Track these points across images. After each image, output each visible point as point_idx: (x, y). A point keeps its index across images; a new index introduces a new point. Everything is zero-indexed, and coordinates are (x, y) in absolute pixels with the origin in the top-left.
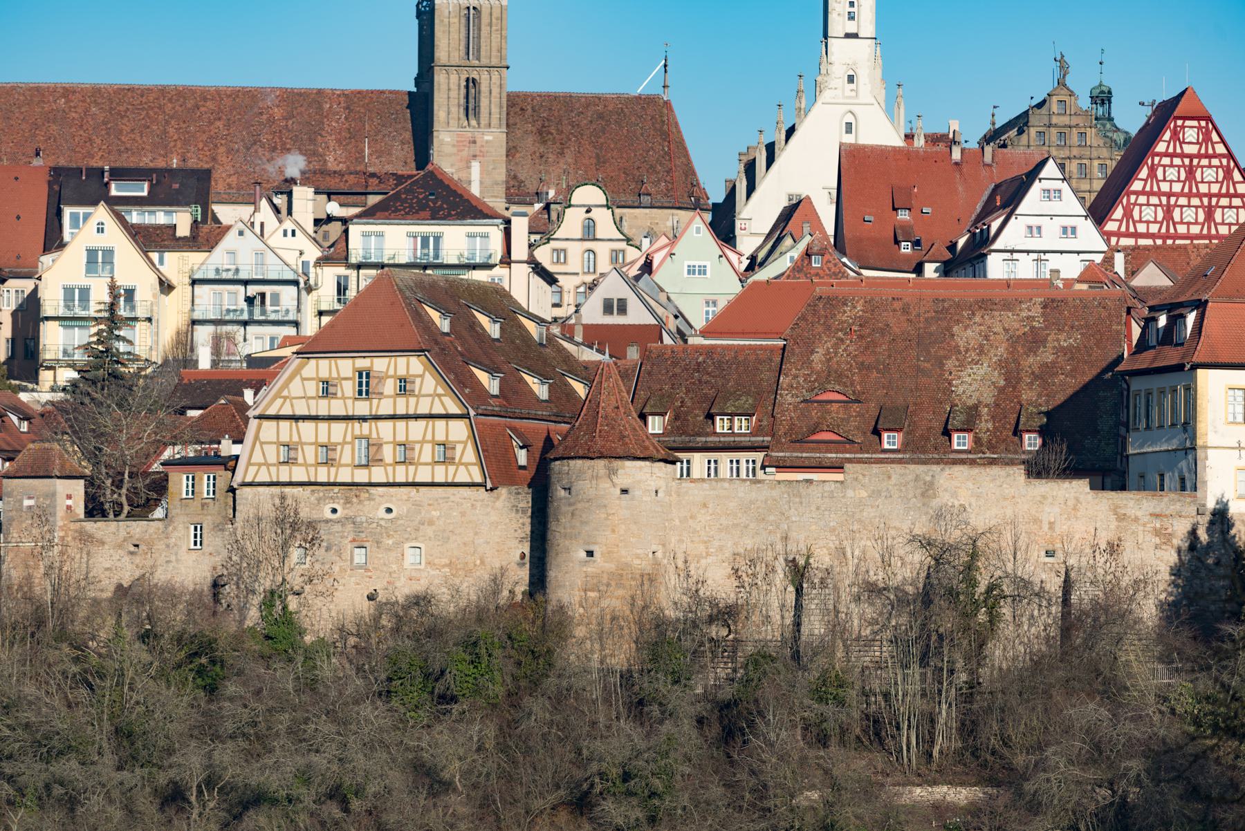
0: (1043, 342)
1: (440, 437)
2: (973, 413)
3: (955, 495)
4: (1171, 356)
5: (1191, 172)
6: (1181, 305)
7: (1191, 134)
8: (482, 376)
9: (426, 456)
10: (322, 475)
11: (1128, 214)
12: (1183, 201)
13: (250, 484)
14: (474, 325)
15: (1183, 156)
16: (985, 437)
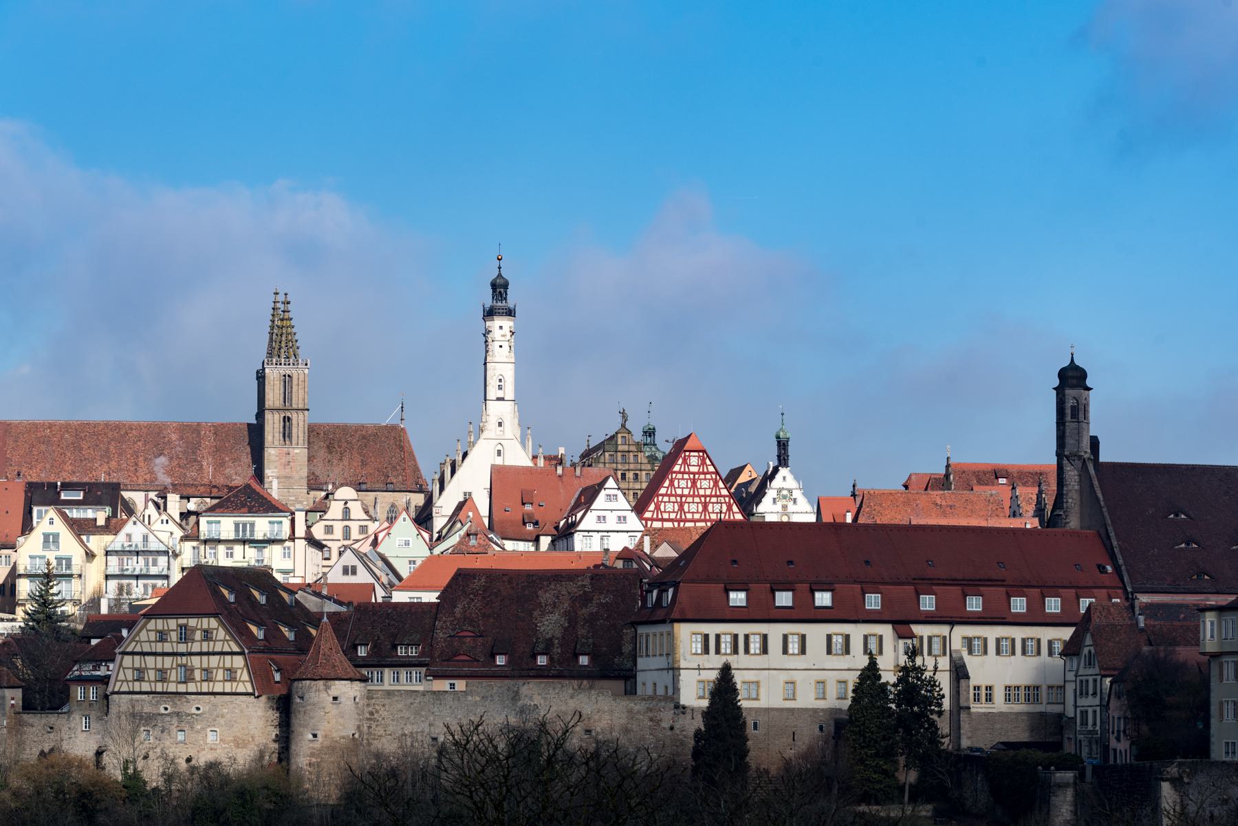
0: (592, 600)
1: (228, 665)
2: (549, 643)
3: (531, 698)
5: (694, 482)
6: (665, 583)
7: (694, 461)
8: (254, 629)
9: (220, 676)
10: (159, 687)
11: (657, 507)
12: (690, 500)
13: (118, 693)
15: (689, 473)
16: (556, 657)
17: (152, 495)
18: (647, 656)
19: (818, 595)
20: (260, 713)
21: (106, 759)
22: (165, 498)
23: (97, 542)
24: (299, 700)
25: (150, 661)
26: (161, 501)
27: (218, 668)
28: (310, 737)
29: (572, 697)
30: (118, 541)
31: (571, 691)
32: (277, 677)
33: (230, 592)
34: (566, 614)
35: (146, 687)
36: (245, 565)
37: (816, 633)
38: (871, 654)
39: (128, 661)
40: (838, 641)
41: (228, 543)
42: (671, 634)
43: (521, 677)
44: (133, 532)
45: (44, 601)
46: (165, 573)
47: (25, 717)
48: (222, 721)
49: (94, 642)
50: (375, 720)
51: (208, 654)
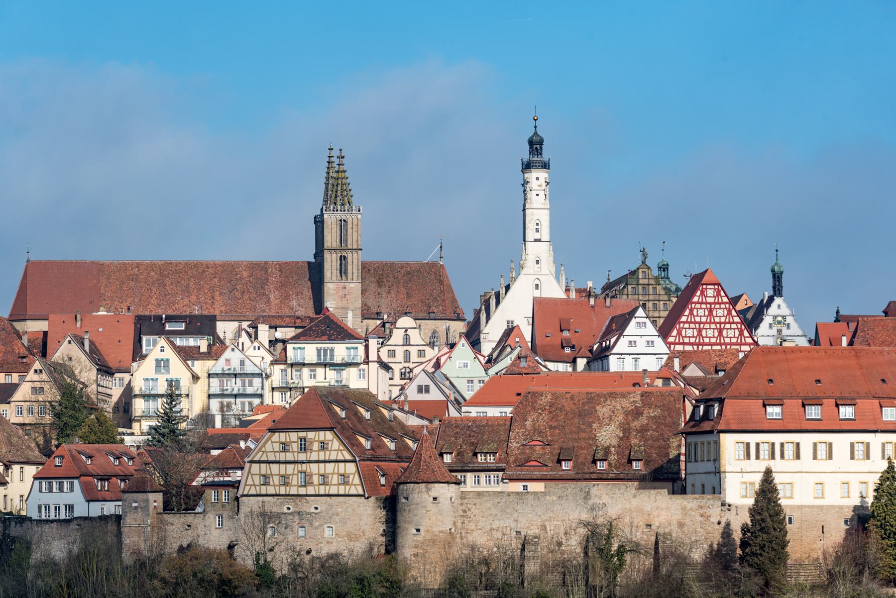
1: (342, 471)
2: (607, 450)
4: (707, 426)
6: (711, 400)
8: (362, 440)
9: (335, 481)
14: (357, 414)
16: (613, 463)
17: (245, 325)
18: (696, 461)
19: (842, 409)
20: (370, 511)
21: (237, 551)
22: (256, 328)
23: (201, 367)
24: (404, 500)
25: (275, 467)
26: (251, 330)
27: (333, 474)
28: (415, 531)
29: (635, 497)
30: (218, 366)
31: (634, 491)
32: (383, 481)
33: (342, 409)
34: (621, 425)
35: (271, 490)
36: (327, 385)
37: (842, 441)
38: (889, 459)
39: (255, 468)
40: (859, 450)
41: (314, 368)
42: (717, 443)
43: (586, 479)
44: (231, 359)
45: (169, 418)
46: (259, 392)
47: (166, 517)
48: (337, 519)
49: (215, 452)
50: (467, 517)
51: (325, 462)
